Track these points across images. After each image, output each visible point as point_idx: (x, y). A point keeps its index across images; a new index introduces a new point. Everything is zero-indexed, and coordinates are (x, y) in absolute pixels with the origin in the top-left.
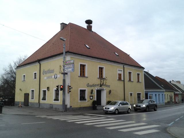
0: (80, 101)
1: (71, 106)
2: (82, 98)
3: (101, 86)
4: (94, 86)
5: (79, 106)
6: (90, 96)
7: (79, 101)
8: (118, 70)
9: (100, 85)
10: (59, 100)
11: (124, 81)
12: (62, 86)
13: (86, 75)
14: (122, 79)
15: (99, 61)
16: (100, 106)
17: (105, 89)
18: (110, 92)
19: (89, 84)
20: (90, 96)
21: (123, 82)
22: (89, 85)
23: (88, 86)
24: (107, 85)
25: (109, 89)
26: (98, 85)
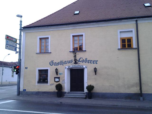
0: (38, 84)
1: (25, 90)
2: (42, 81)
3: (76, 63)
4: (62, 63)
5: (37, 91)
6: (55, 78)
7: (37, 84)
8: (120, 32)
9: (74, 62)
10: (49, 82)
11: (138, 49)
12: (18, 66)
13: (84, 50)
14: (134, 45)
15: (71, 27)
16: (83, 92)
17: (84, 67)
18: (95, 70)
19: (54, 62)
20: (55, 78)
21: (136, 52)
22: (53, 63)
23: (52, 64)
24: (91, 61)
25: (93, 66)
26: (69, 62)
